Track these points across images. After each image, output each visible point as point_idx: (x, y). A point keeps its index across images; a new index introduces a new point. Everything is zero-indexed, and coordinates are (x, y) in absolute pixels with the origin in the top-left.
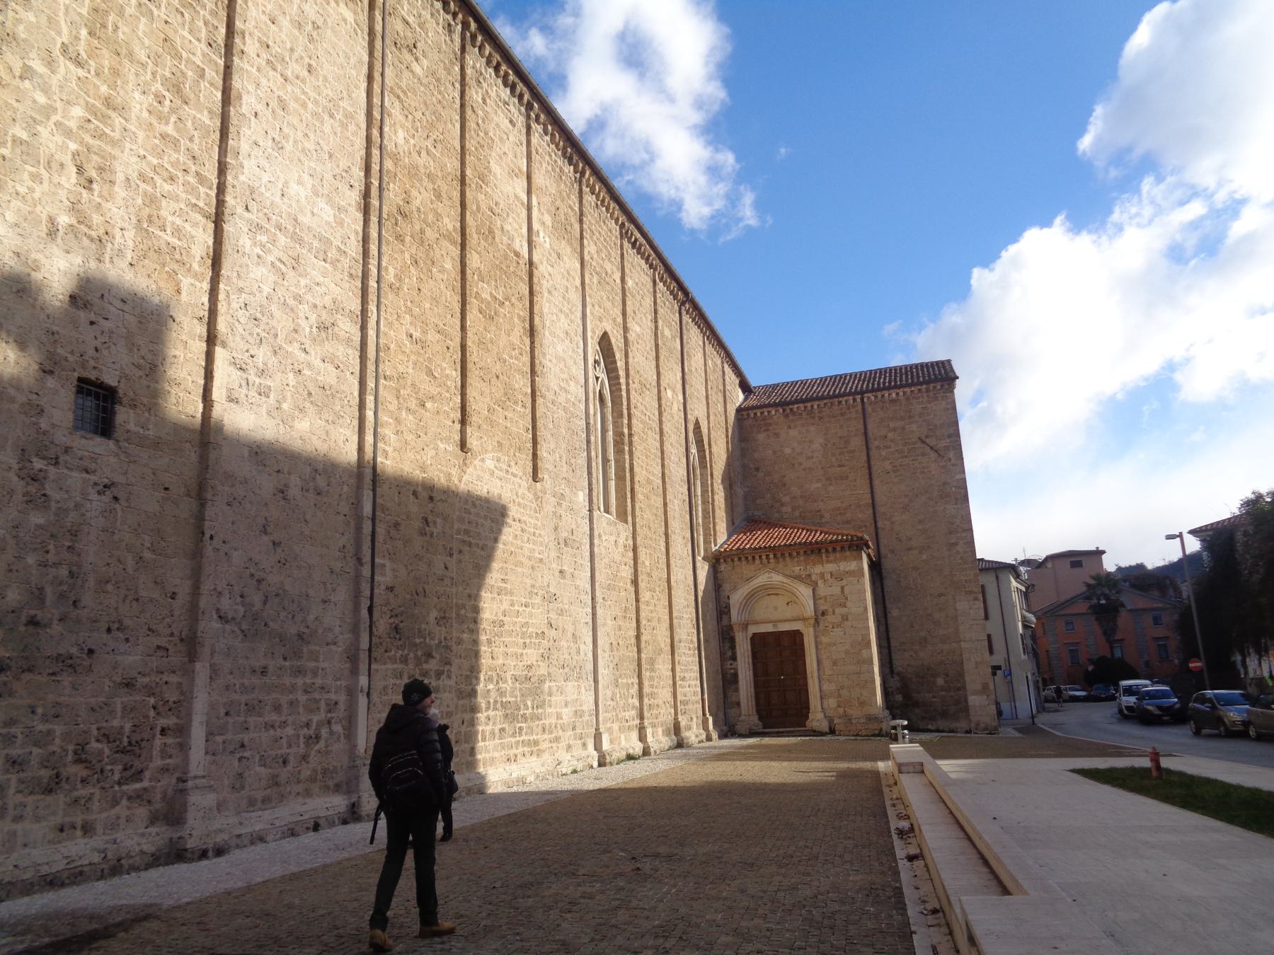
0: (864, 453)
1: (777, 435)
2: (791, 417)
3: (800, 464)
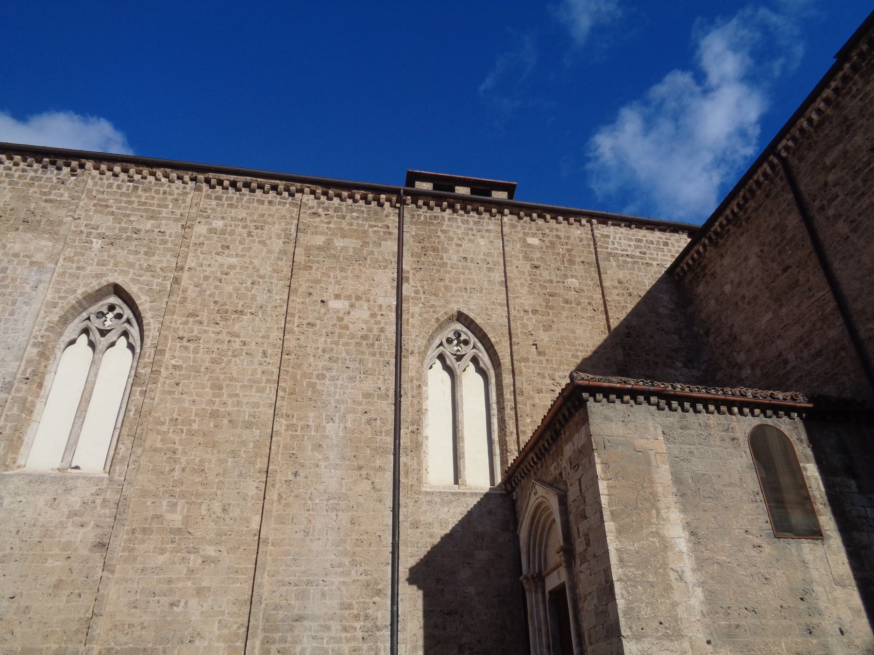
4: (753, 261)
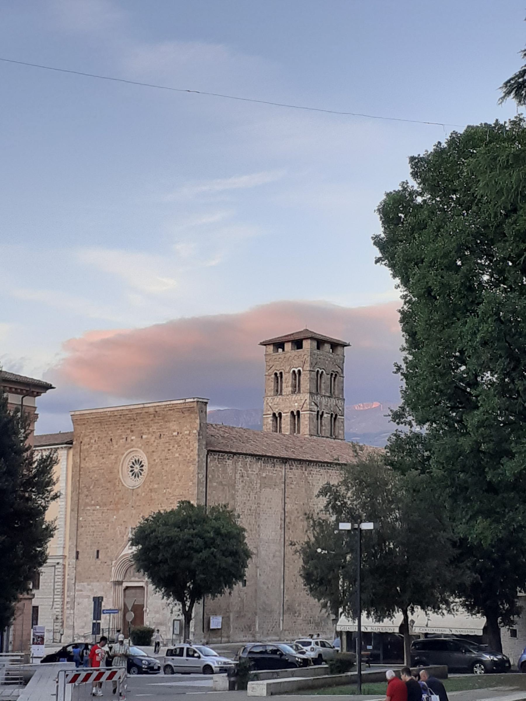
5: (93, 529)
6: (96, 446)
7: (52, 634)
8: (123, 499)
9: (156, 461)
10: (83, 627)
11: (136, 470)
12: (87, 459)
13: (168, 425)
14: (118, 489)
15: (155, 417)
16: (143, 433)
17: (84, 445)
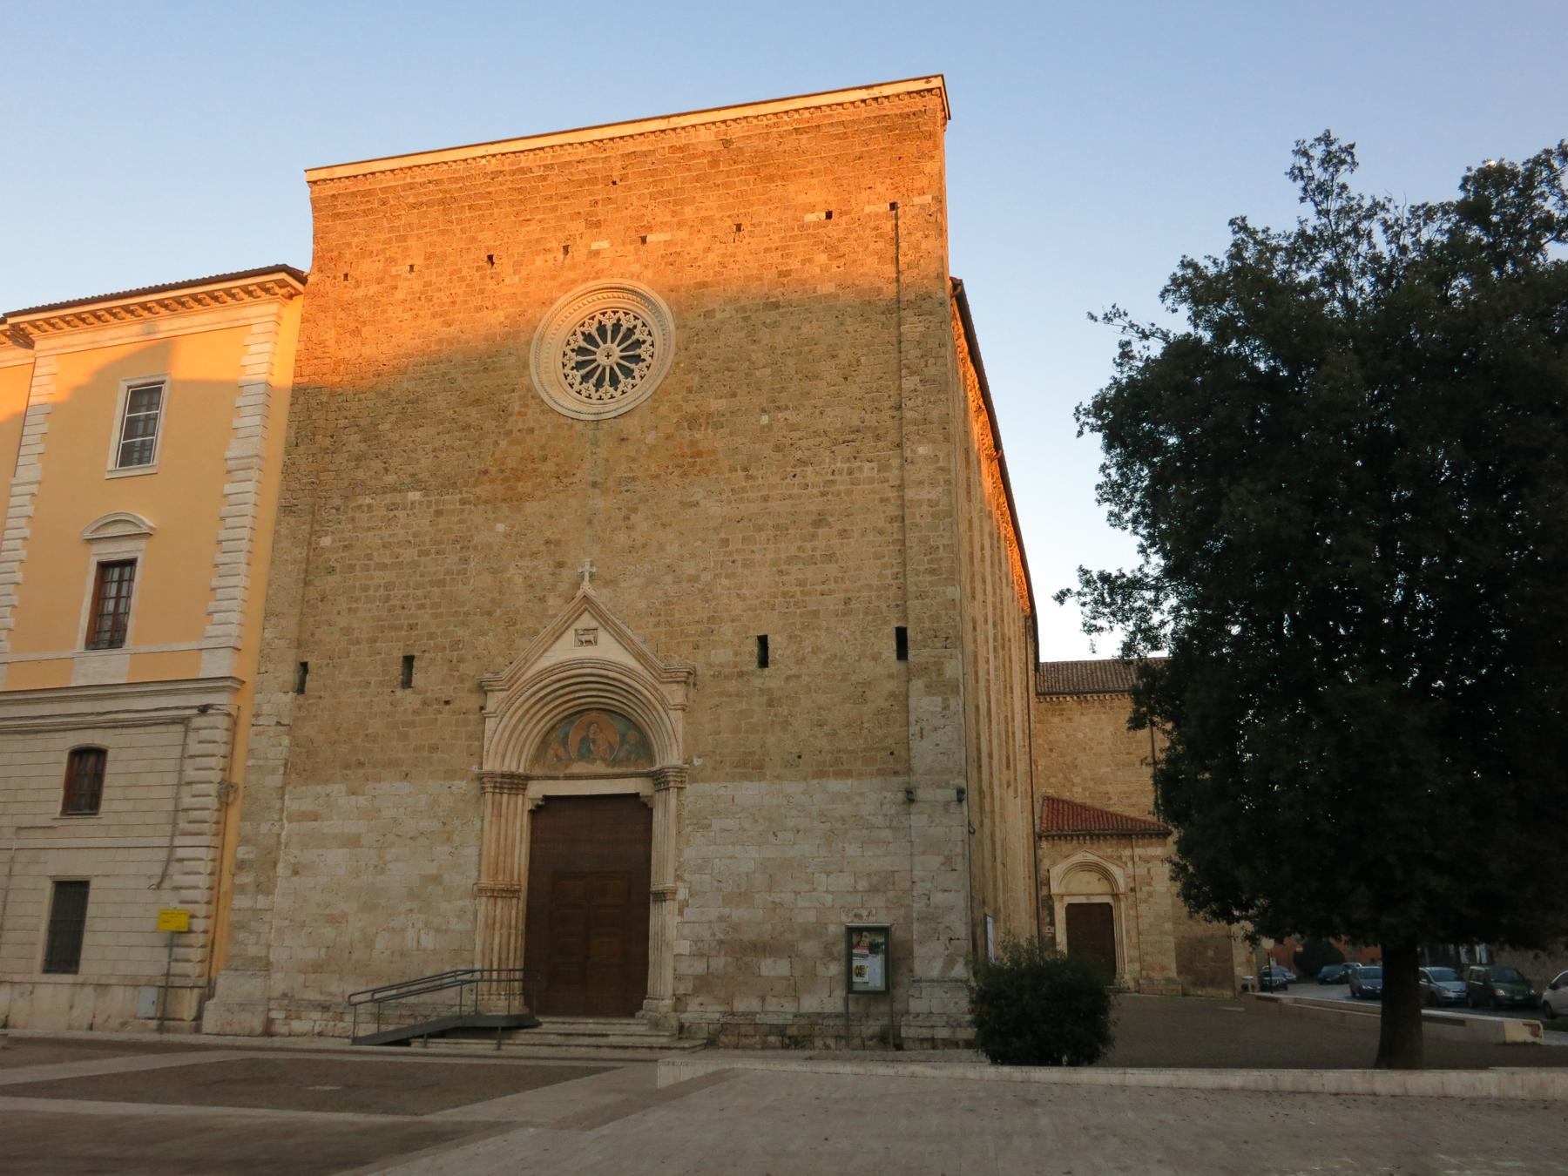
0: (1150, 744)
1: (1070, 719)
2: (1083, 705)
3: (1091, 749)
4: (1107, 733)
5: (380, 577)
6: (418, 285)
7: (151, 994)
8: (545, 459)
9: (719, 316)
10: (317, 967)
11: (601, 359)
12: (366, 331)
13: (775, 189)
14: (520, 426)
15: (714, 163)
16: (650, 229)
17: (358, 284)
